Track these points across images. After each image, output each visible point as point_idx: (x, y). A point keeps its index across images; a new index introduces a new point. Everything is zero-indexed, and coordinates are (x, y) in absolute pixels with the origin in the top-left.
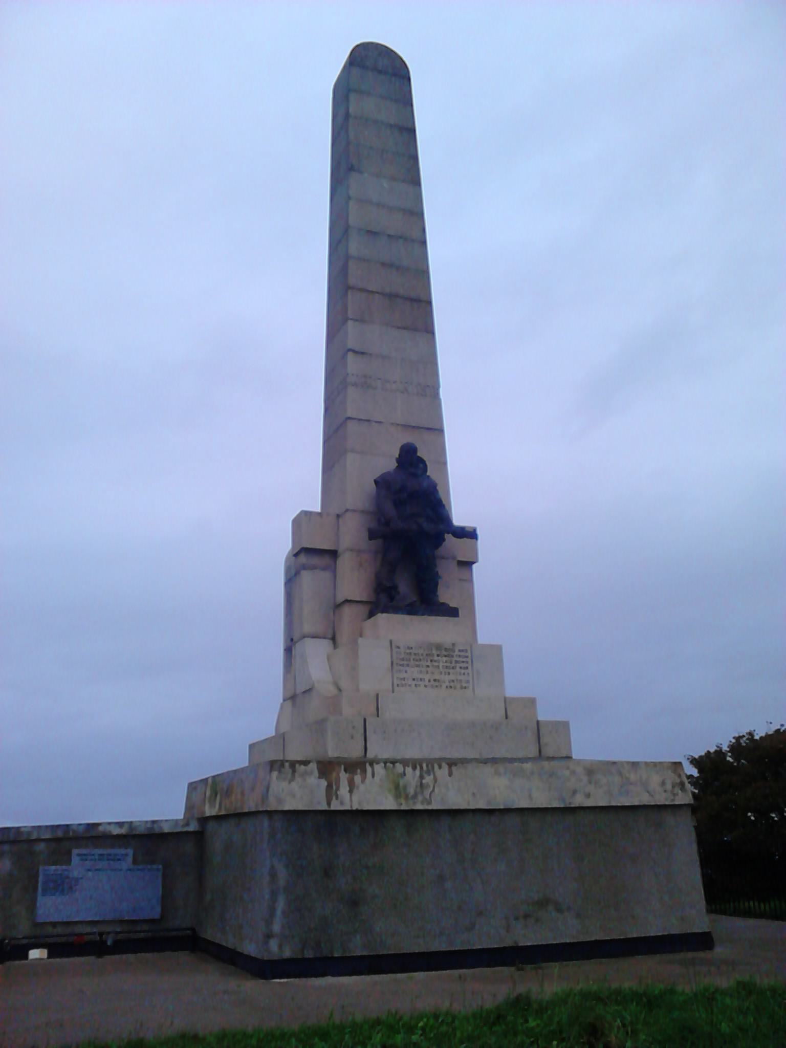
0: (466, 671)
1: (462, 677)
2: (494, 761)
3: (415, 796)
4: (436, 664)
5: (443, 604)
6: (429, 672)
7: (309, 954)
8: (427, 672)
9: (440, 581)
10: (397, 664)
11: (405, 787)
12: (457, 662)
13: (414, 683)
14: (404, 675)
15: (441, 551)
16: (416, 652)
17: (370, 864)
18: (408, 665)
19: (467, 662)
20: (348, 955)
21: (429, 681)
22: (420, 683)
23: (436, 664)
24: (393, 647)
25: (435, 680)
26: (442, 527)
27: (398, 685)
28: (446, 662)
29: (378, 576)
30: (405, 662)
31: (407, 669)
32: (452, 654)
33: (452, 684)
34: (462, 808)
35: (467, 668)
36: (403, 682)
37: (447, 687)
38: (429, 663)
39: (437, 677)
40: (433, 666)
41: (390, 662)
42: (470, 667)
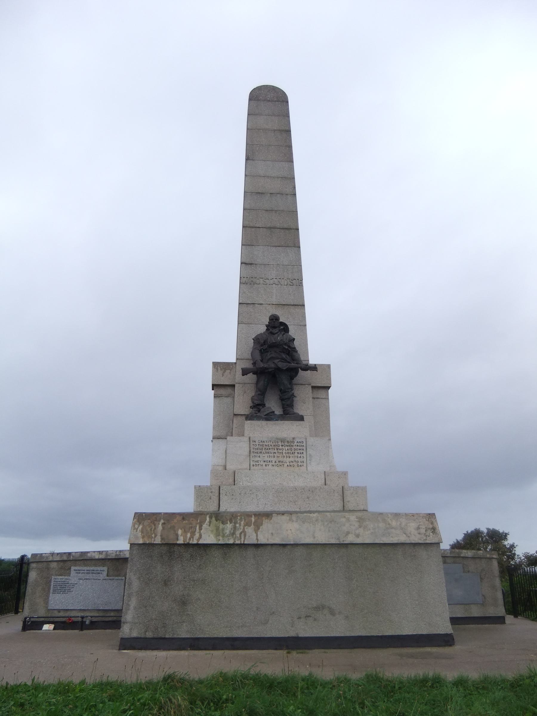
0: (302, 455)
1: (299, 459)
2: (290, 513)
3: (228, 536)
4: (280, 451)
5: (294, 413)
6: (276, 456)
7: (149, 635)
8: (274, 457)
9: (295, 399)
10: (253, 452)
11: (223, 529)
12: (295, 450)
13: (264, 464)
14: (258, 459)
15: (295, 381)
16: (267, 444)
17: (195, 579)
18: (261, 452)
19: (303, 450)
20: (175, 636)
21: (275, 462)
22: (268, 463)
23: (280, 451)
24: (251, 442)
25: (279, 462)
26: (293, 365)
27: (253, 465)
28: (288, 450)
29: (252, 399)
30: (259, 451)
31: (261, 455)
32: (292, 444)
33: (291, 464)
34: (262, 543)
35: (303, 453)
36: (257, 463)
37: (288, 466)
38: (276, 451)
39: (281, 459)
40: (278, 452)
41: (248, 451)
42: (305, 453)
